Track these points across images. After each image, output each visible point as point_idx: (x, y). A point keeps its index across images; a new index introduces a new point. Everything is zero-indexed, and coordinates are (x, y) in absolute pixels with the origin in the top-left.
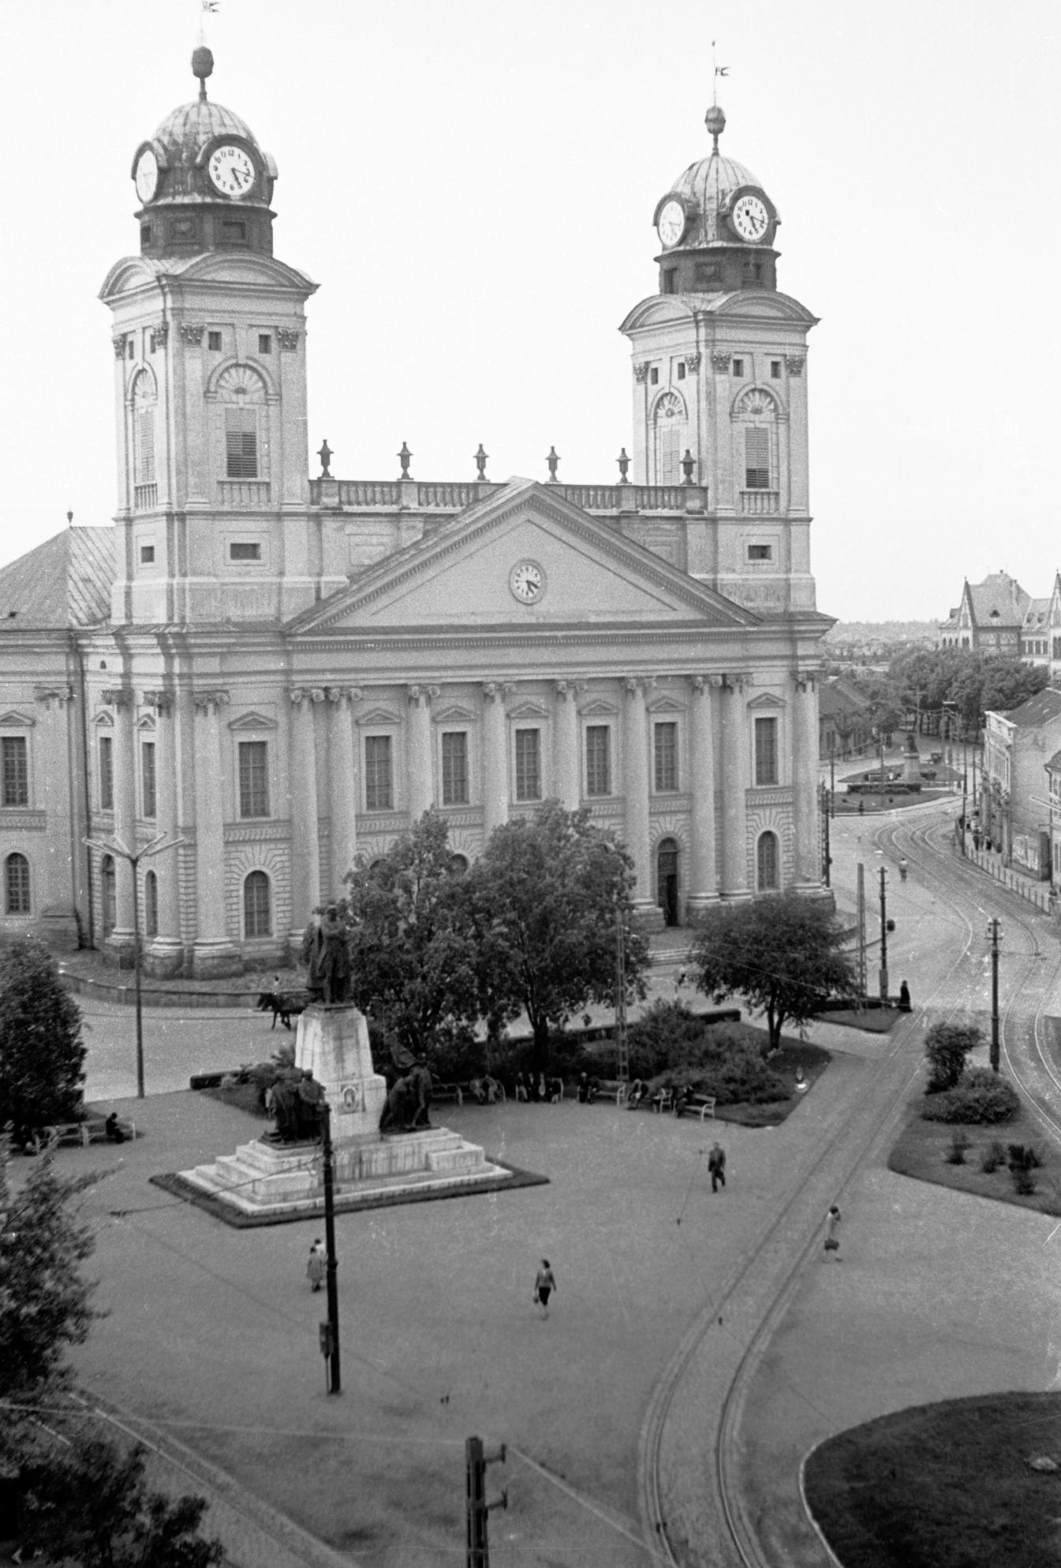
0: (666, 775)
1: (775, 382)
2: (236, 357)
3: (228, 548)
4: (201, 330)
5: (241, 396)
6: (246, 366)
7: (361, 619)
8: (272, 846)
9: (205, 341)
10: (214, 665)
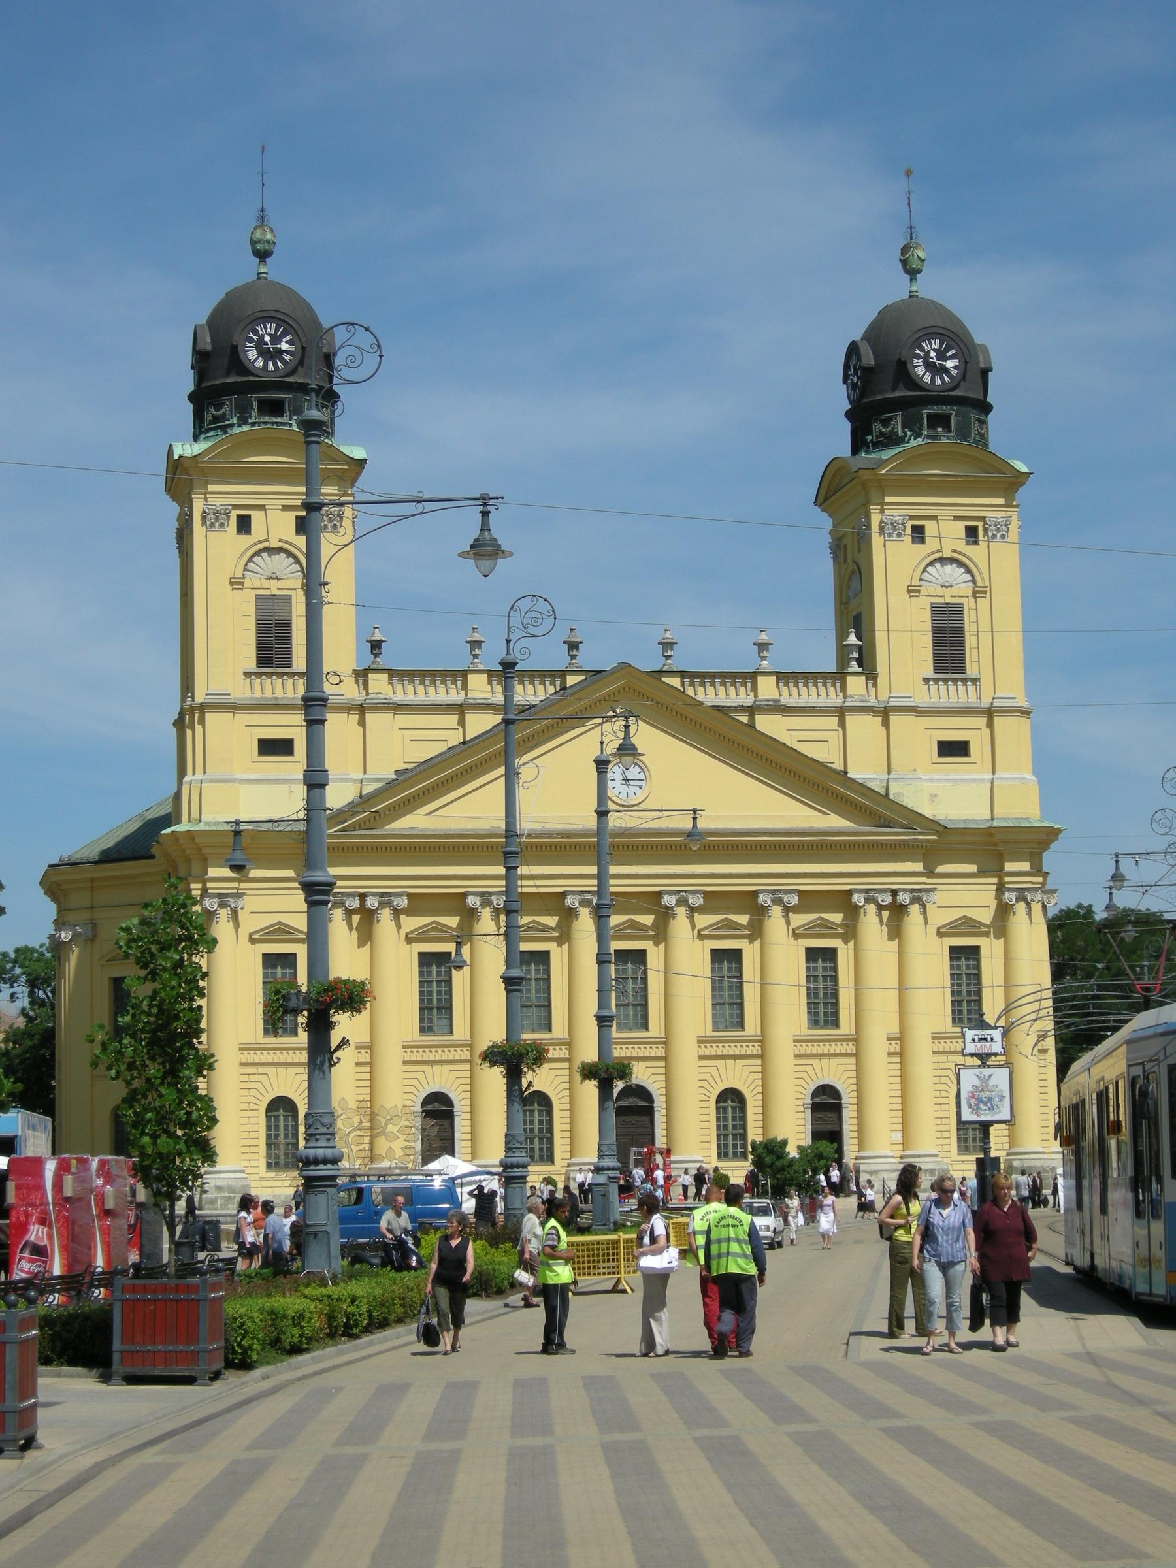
0: (823, 1007)
1: (970, 550)
4: (227, 515)
7: (415, 821)
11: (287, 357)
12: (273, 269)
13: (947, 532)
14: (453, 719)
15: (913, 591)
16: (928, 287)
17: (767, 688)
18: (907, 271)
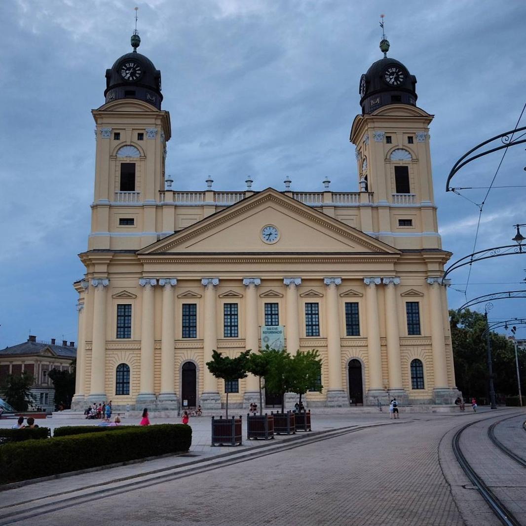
0: (353, 326)
3: (119, 220)
5: (128, 158)
8: (132, 352)
10: (104, 268)
11: (137, 75)
12: (139, 50)
13: (400, 139)
14: (198, 211)
15: (387, 160)
16: (390, 55)
17: (328, 200)
18: (383, 51)
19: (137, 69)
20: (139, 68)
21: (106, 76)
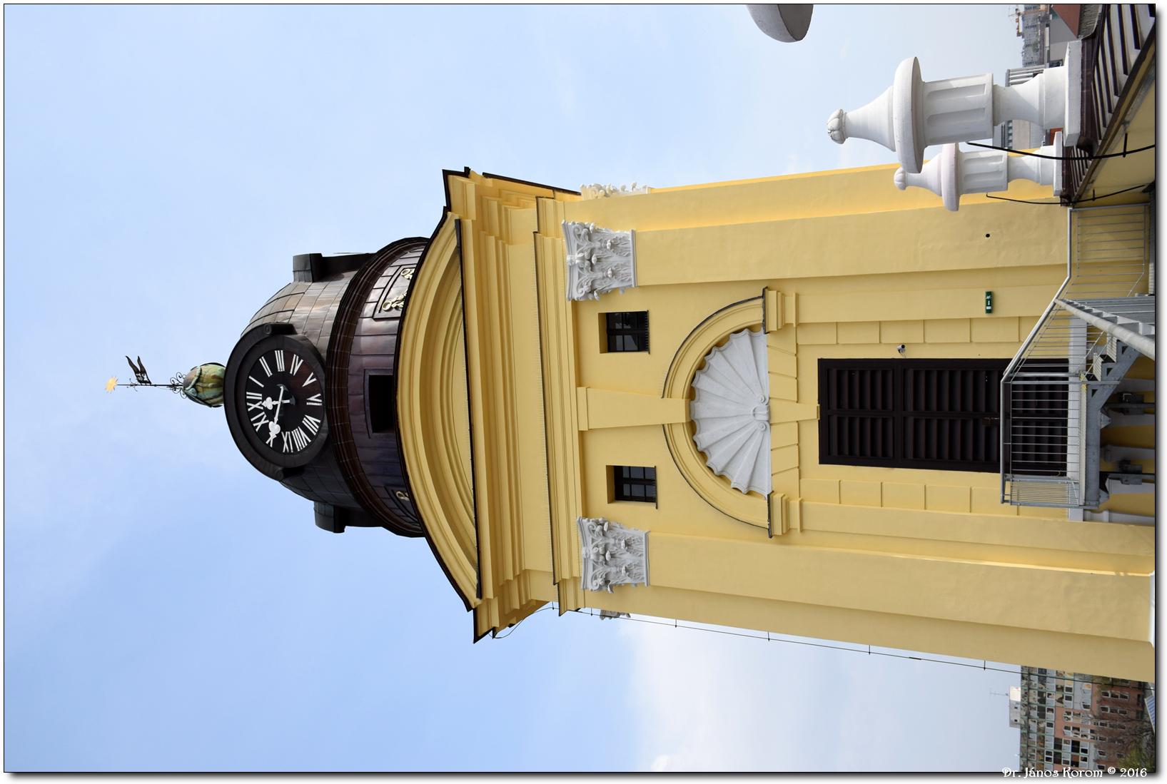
2: (666, 430)
6: (692, 394)
9: (631, 514)
11: (296, 366)
19: (269, 373)
20: (263, 361)
21: (339, 529)
